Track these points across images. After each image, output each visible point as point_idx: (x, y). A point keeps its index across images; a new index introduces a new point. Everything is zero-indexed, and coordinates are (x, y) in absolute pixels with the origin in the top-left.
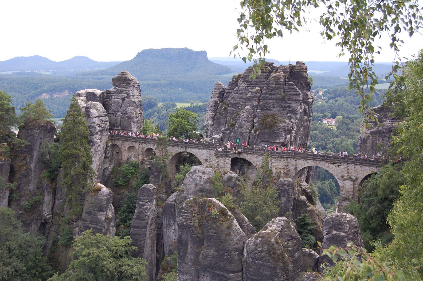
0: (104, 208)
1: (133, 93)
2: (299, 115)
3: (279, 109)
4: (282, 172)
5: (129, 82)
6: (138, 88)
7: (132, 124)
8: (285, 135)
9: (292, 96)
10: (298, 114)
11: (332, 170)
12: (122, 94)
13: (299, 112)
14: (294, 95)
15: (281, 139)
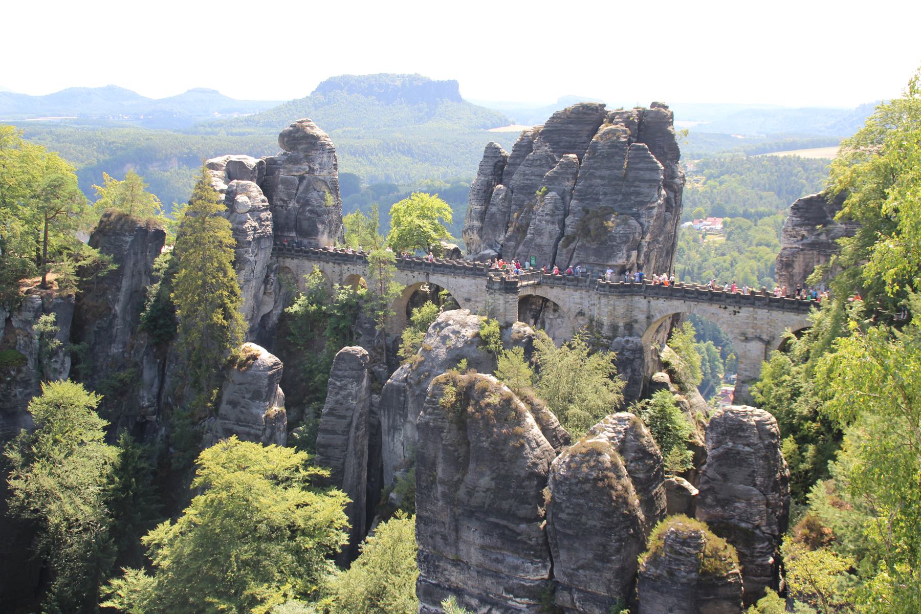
0: (264, 394)
1: (320, 164)
2: (655, 211)
3: (615, 197)
4: (621, 324)
5: (313, 141)
6: (332, 155)
7: (320, 227)
8: (629, 250)
9: (642, 173)
10: (653, 208)
11: (720, 321)
12: (299, 166)
13: (656, 204)
14: (647, 169)
15: (620, 258)
